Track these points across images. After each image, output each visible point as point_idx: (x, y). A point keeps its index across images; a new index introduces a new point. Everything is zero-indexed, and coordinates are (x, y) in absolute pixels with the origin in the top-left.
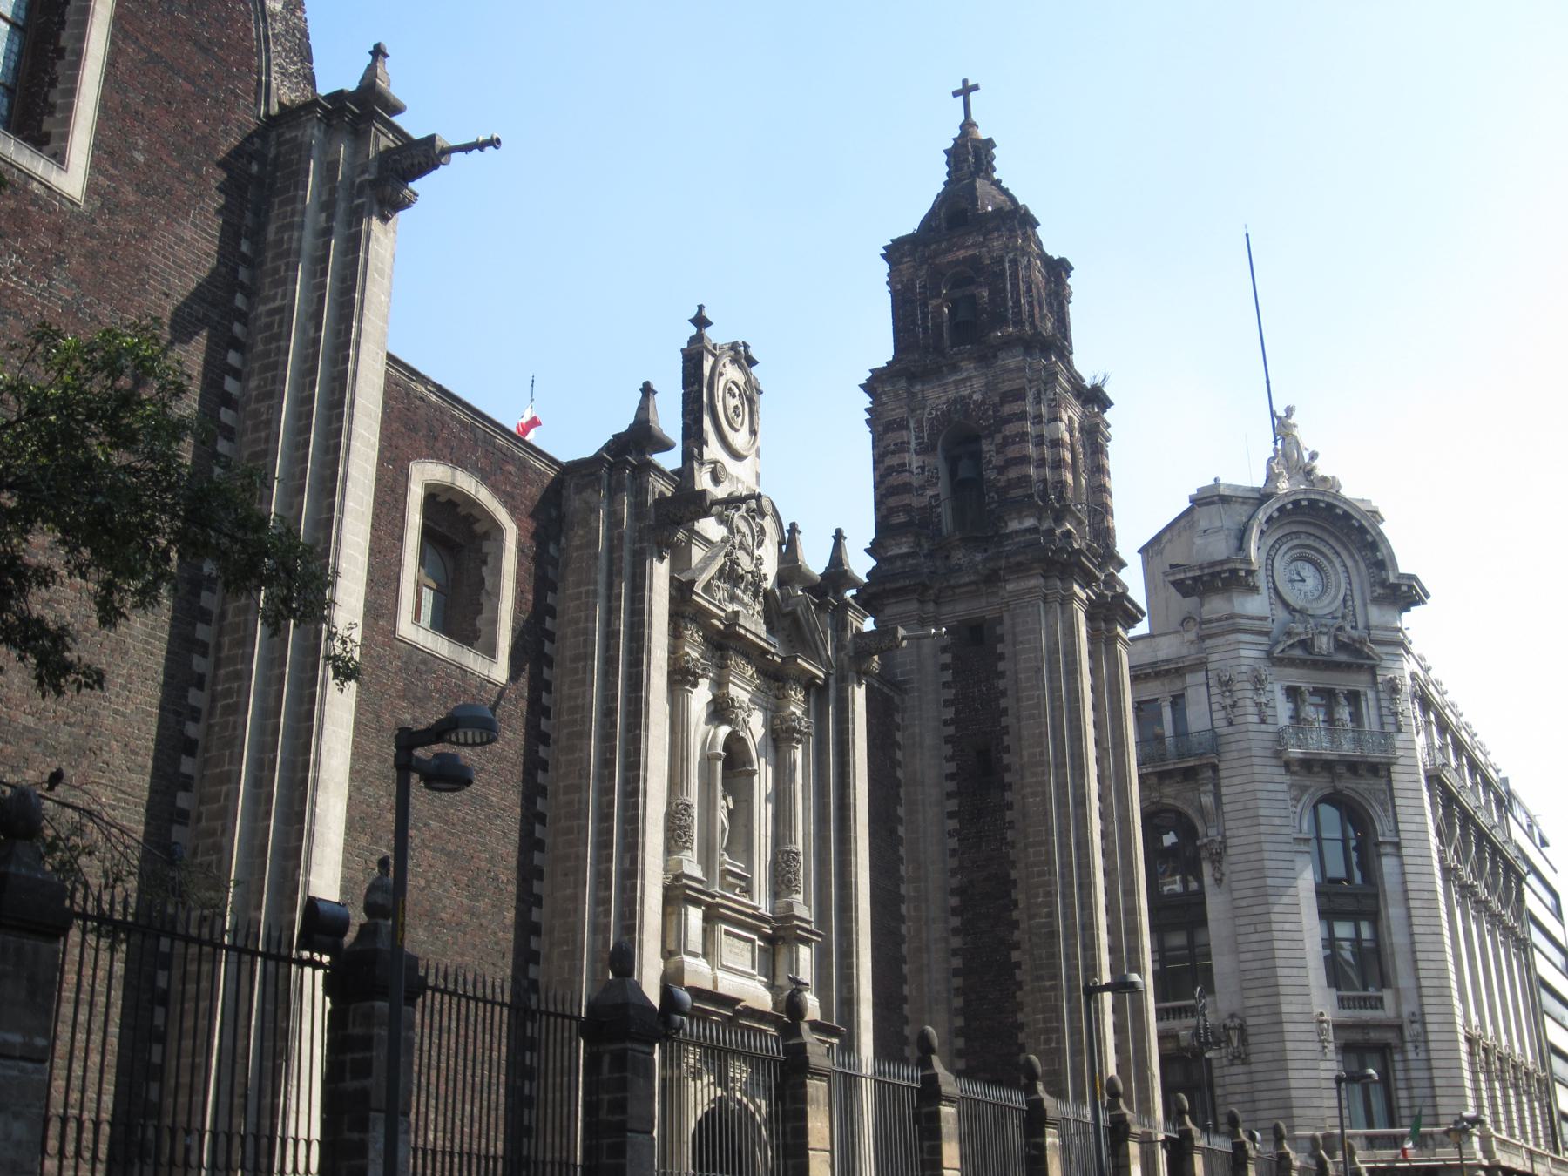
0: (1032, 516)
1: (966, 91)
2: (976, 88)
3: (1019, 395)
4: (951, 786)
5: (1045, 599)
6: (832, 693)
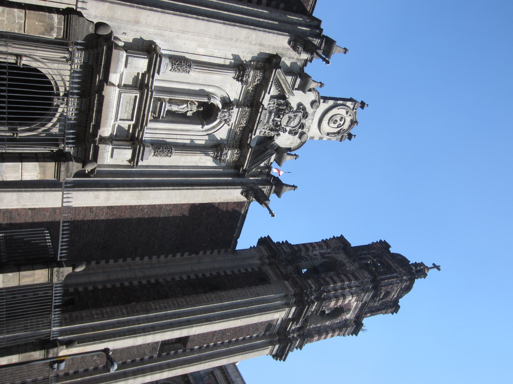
0: (316, 287)
1: (436, 267)
2: (439, 269)
3: (356, 279)
4: (200, 275)
5: (286, 296)
6: (237, 180)
